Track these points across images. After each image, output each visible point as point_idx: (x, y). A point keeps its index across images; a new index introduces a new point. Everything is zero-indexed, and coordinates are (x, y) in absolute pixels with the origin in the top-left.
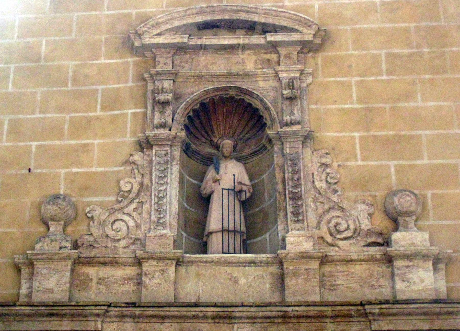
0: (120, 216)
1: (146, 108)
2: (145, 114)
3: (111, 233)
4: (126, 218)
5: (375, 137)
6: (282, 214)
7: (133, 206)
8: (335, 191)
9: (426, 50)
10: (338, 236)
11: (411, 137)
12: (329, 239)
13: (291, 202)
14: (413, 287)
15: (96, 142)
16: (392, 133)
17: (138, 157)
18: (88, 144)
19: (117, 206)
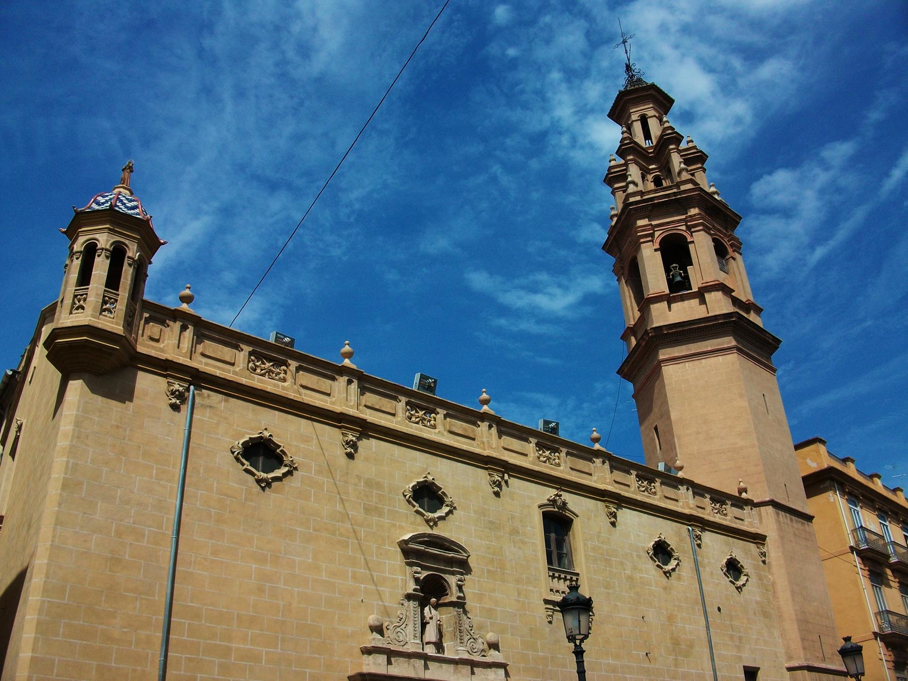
0: (398, 629)
1: (406, 576)
2: (406, 580)
3: (397, 638)
4: (402, 631)
5: (483, 607)
6: (456, 638)
7: (404, 626)
8: (471, 630)
9: (499, 570)
10: (474, 651)
11: (494, 609)
12: (471, 652)
13: (459, 634)
14: (499, 678)
15: (387, 590)
16: (489, 607)
17: (406, 603)
18: (384, 590)
19: (397, 624)
